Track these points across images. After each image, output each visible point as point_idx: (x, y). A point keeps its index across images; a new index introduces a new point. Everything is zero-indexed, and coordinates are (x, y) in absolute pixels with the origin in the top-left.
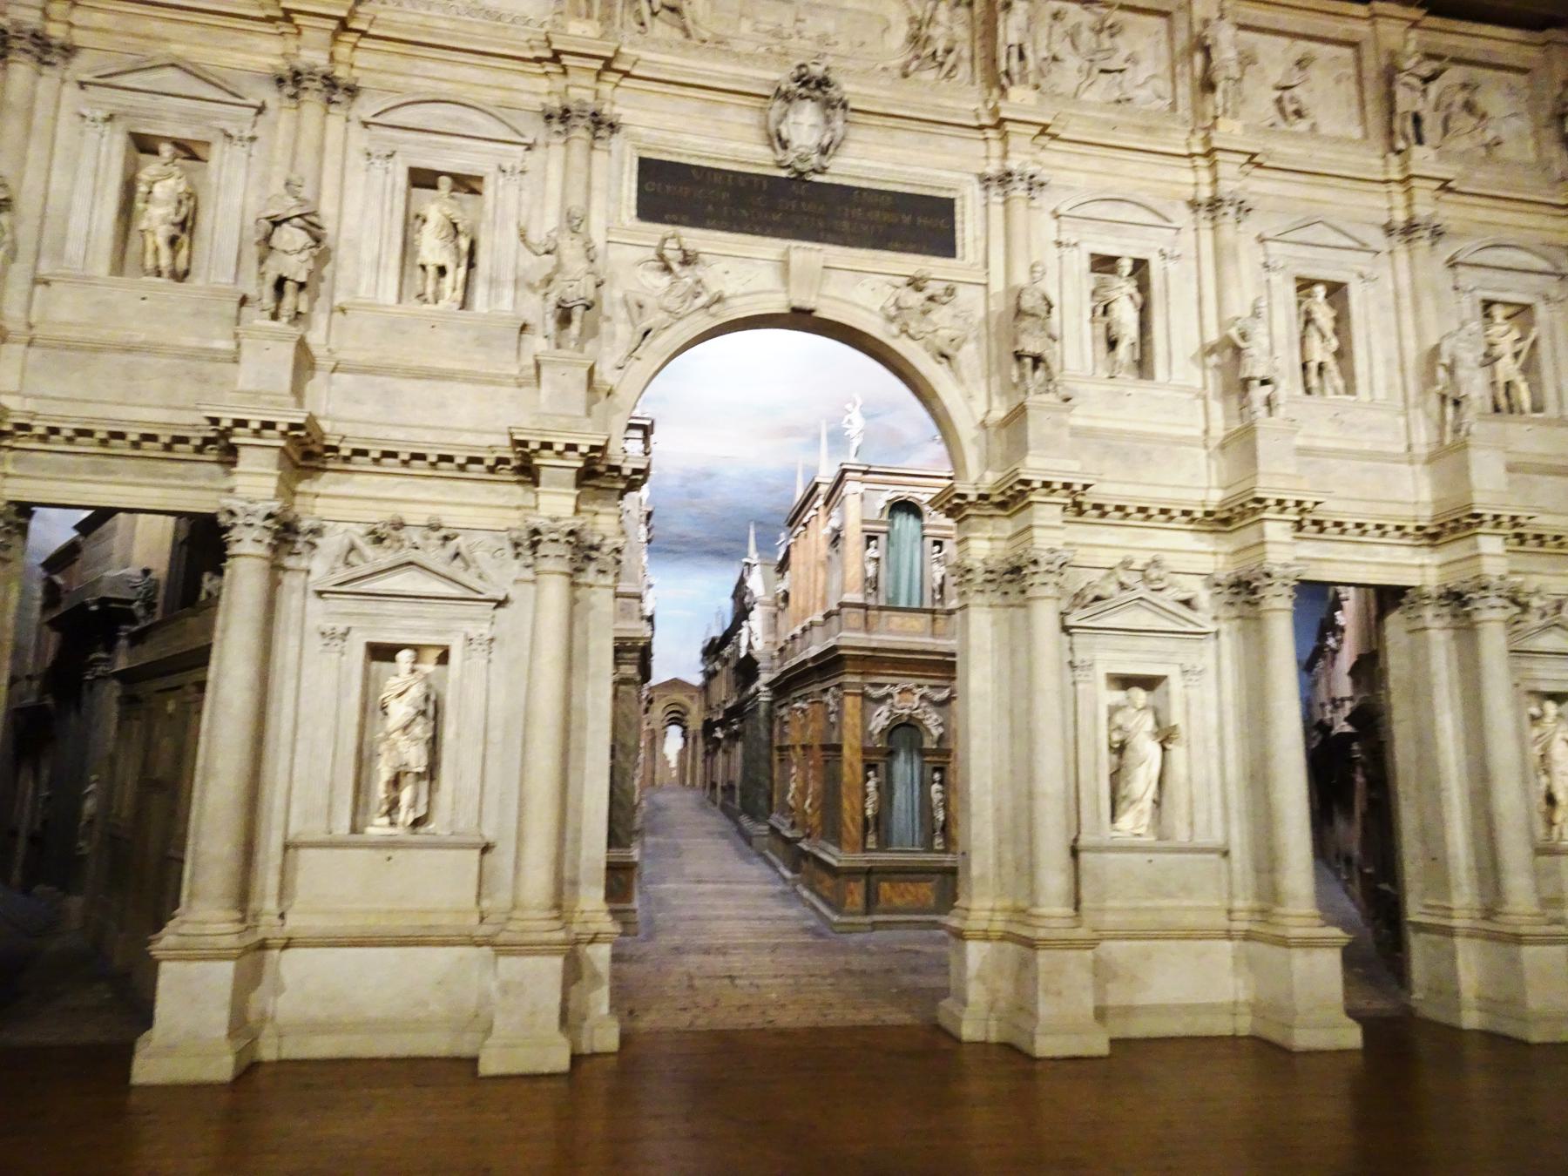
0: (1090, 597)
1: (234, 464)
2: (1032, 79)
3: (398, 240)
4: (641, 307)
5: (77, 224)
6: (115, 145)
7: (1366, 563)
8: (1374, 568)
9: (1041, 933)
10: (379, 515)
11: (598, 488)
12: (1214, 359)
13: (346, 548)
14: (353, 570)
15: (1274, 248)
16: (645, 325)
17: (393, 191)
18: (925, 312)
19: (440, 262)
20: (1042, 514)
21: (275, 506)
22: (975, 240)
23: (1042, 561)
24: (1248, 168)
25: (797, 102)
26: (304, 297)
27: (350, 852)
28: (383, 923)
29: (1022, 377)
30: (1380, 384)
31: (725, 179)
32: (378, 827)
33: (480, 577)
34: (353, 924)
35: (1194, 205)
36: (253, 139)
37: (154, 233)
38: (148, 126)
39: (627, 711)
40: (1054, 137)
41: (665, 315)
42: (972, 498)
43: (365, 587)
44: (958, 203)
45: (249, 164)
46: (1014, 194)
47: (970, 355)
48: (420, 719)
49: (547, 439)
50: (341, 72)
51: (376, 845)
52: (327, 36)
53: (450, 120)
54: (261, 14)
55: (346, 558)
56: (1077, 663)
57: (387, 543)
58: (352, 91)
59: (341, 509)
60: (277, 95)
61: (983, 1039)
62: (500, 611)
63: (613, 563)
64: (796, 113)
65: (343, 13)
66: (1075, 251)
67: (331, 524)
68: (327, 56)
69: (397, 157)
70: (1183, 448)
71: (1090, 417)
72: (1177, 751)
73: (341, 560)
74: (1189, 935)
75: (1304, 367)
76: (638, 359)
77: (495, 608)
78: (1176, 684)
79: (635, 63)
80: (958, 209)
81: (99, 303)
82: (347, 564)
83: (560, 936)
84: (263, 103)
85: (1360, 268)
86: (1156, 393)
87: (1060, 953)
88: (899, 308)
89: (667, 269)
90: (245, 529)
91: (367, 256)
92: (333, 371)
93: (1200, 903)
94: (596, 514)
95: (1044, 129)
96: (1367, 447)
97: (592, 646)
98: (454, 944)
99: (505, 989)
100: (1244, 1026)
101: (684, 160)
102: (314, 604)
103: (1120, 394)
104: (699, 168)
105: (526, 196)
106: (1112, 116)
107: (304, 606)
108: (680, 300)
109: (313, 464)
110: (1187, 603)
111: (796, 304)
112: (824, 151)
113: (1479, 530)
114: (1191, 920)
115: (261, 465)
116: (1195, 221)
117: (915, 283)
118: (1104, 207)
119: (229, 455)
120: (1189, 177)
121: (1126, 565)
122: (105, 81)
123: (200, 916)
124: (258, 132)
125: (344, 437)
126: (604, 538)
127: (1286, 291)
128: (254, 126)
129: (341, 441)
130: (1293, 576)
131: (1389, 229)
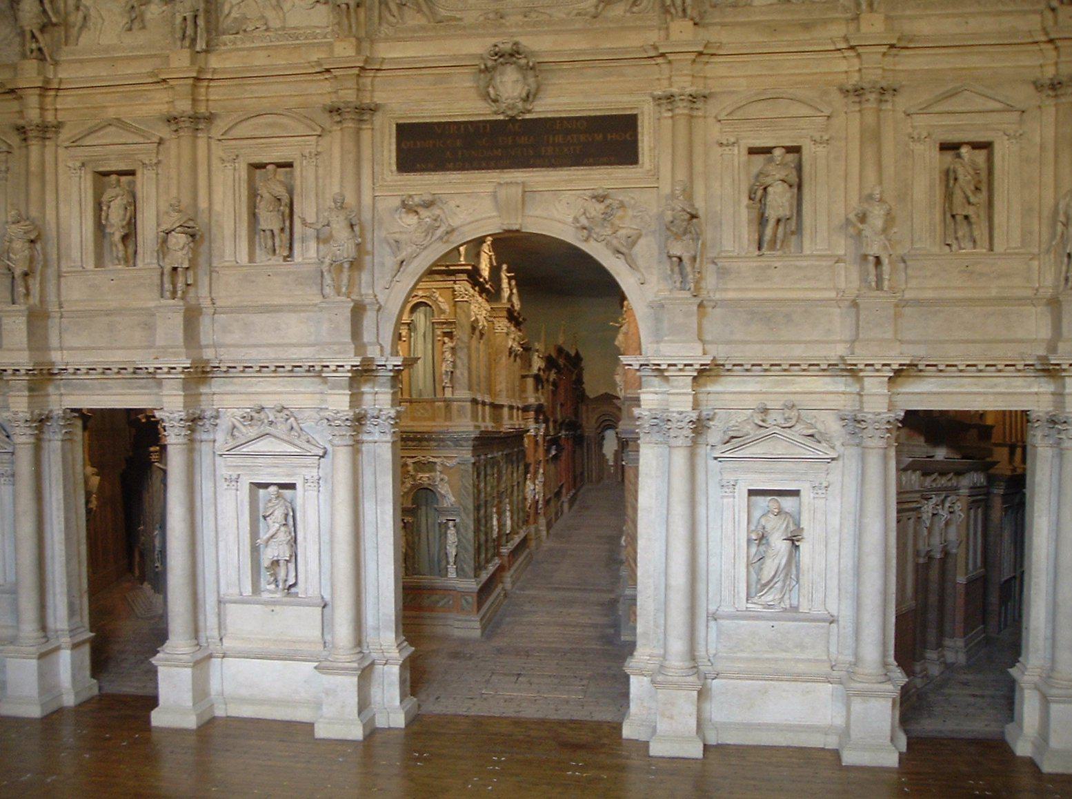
0: (727, 438)
2: (689, 11)
3: (245, 217)
5: (75, 238)
6: (88, 183)
7: (984, 394)
8: (991, 398)
9: (660, 678)
12: (851, 230)
13: (230, 428)
15: (920, 121)
16: (400, 258)
17: (239, 183)
18: (607, 216)
19: (270, 227)
20: (675, 384)
21: (183, 415)
22: (650, 150)
24: (894, 51)
25: (500, 67)
26: (190, 273)
28: (272, 647)
29: (672, 270)
30: (1016, 235)
31: (459, 129)
33: (308, 442)
35: (845, 92)
36: (159, 162)
37: (113, 234)
38: (103, 166)
39: (467, 485)
40: (712, 55)
43: (245, 450)
44: (640, 117)
45: (158, 180)
46: (678, 111)
47: (646, 248)
48: (283, 529)
49: (325, 364)
50: (202, 109)
51: (266, 603)
52: (188, 89)
53: (271, 125)
54: (150, 80)
56: (724, 483)
58: (210, 118)
60: (168, 129)
62: (322, 459)
63: (390, 426)
64: (500, 74)
65: (194, 75)
66: (736, 149)
68: (190, 103)
69: (241, 158)
70: (819, 308)
71: (740, 290)
72: (803, 546)
74: (797, 678)
75: (953, 216)
78: (806, 496)
79: (382, 63)
80: (639, 123)
81: (90, 286)
82: (232, 435)
83: (355, 665)
84: (161, 139)
85: (1005, 126)
86: (798, 263)
88: (587, 218)
89: (417, 213)
91: (228, 231)
93: (811, 657)
94: (376, 393)
95: (700, 54)
96: (994, 293)
97: (379, 482)
98: (309, 661)
99: (327, 693)
100: (831, 742)
101: (428, 120)
102: (218, 459)
103: (769, 267)
104: (439, 124)
105: (321, 171)
106: (778, 17)
107: (214, 464)
108: (424, 234)
110: (812, 436)
111: (505, 228)
112: (526, 99)
113: (1063, 374)
114: (801, 667)
116: (846, 105)
117: (600, 198)
118: (760, 105)
119: (159, 383)
120: (843, 65)
121: (765, 411)
122: (75, 143)
124: (160, 158)
126: (381, 410)
127: (931, 160)
128: (158, 153)
130: (884, 421)
131: (1038, 86)
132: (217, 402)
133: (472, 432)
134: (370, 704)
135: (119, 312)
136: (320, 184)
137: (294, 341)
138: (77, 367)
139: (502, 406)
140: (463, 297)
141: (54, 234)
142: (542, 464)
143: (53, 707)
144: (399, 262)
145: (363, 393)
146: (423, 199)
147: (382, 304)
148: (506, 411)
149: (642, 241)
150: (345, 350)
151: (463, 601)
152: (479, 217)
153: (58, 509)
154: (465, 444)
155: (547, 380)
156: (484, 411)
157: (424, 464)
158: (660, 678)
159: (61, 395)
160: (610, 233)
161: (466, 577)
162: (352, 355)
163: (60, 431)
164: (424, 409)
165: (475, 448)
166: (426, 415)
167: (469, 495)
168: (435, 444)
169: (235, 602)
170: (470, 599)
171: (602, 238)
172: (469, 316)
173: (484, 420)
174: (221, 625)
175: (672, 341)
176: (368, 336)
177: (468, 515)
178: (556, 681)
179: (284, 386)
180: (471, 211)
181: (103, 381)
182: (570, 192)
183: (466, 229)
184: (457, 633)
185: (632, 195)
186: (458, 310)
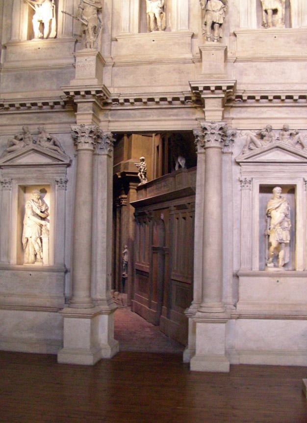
1: (204, 107)
5: (125, 14)
10: (261, 126)
14: (252, 151)
19: (274, 8)
26: (221, 30)
27: (261, 278)
32: (271, 269)
34: (265, 310)
48: (286, 219)
55: (249, 146)
57: (265, 138)
59: (243, 124)
67: (239, 131)
73: (247, 147)
81: (136, 45)
82: (250, 149)
90: (212, 136)
92: (235, 61)
102: (236, 169)
109: (231, 104)
115: (215, 106)
123: (209, 304)
125: (245, 91)
129: (243, 93)
132: (234, 124)
135: (160, 62)
137: (296, 81)
138: (126, 98)
141: (110, 10)
143: (97, 360)
153: (102, 207)
159: (109, 121)
163: (107, 148)
169: (247, 275)
174: (236, 295)
179: (287, 113)
181: (145, 111)
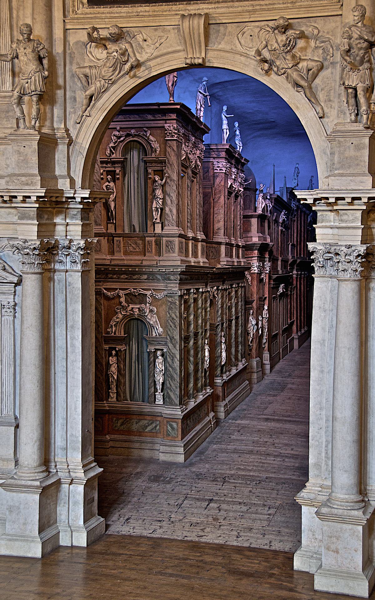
4: (86, 76)
9: (324, 510)
11: (68, 208)
20: (345, 217)
23: (342, 253)
33: (4, 269)
39: (173, 316)
41: (103, 81)
42: (310, 201)
61: (307, 570)
76: (88, 116)
77: (15, 287)
83: (38, 483)
87: (340, 525)
94: (67, 225)
97: (69, 309)
99: (11, 509)
108: (111, 69)
111: (188, 61)
126: (71, 241)
133: (178, 266)
134: (56, 522)
136: (14, 15)
139: (220, 243)
140: (172, 136)
142: (267, 302)
144: (88, 97)
145: (55, 225)
146: (110, 32)
147: (74, 138)
148: (223, 248)
149: (322, 74)
150: (32, 182)
151: (169, 427)
152: (165, 51)
154: (172, 277)
155: (276, 221)
156: (195, 247)
157: (135, 296)
158: (324, 510)
160: (290, 66)
161: (172, 403)
162: (39, 187)
164: (136, 243)
165: (182, 282)
166: (137, 250)
167: (175, 327)
168: (145, 277)
170: (175, 425)
171: (283, 71)
172: (179, 155)
173: (195, 255)
175: (341, 175)
176: (60, 170)
177: (175, 347)
178: (244, 508)
180: (157, 45)
182: (253, 24)
183: (151, 63)
184: (162, 457)
185: (316, 25)
186: (168, 149)
